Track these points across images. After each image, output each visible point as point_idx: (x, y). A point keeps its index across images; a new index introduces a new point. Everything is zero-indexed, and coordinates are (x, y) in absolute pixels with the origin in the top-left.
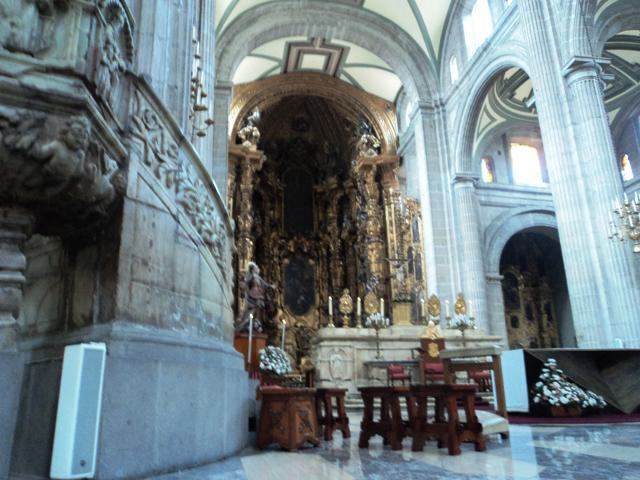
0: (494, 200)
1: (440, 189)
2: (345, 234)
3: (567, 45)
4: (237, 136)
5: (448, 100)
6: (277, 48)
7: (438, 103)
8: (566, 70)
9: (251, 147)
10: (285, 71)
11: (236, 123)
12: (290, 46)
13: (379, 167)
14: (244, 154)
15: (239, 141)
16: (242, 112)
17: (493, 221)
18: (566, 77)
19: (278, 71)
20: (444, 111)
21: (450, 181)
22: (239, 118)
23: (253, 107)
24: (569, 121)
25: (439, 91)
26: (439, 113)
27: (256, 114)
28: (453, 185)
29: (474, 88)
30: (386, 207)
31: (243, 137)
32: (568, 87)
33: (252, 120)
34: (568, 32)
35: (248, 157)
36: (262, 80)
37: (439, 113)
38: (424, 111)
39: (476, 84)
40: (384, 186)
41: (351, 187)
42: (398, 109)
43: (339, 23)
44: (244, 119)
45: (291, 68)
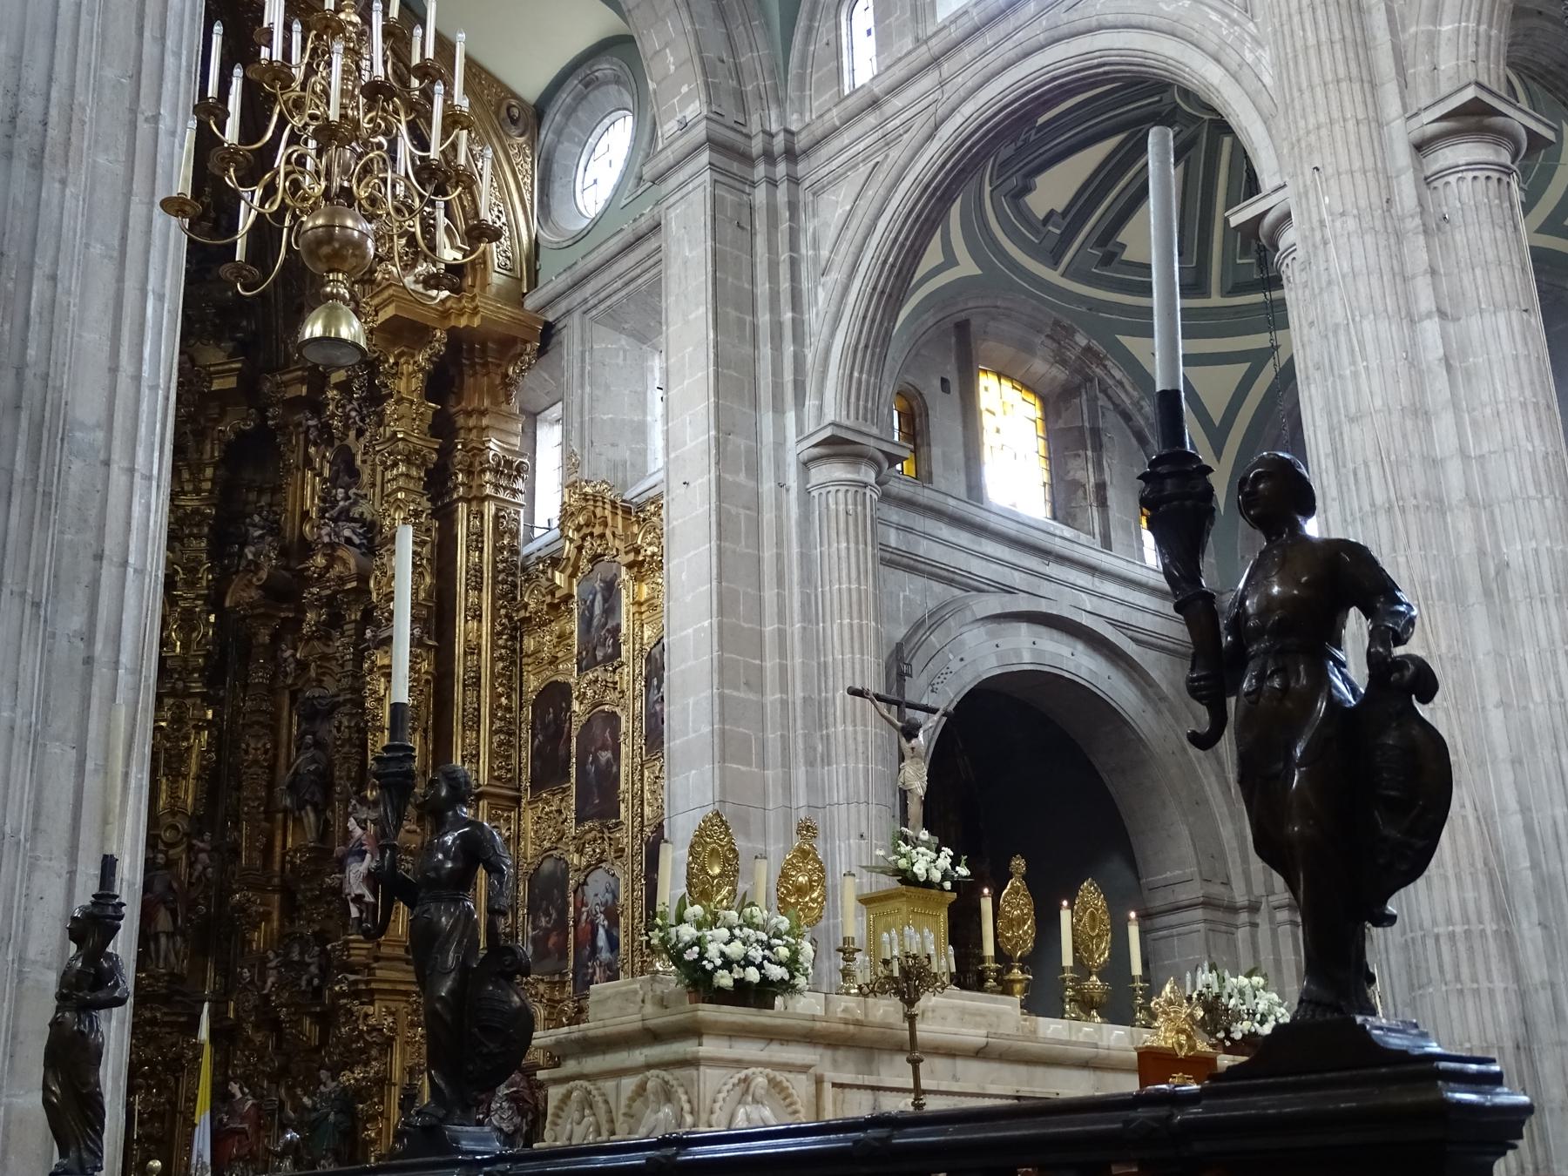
0: (924, 548)
1: (754, 471)
2: (241, 594)
3: (1432, 41)
5: (818, 143)
7: (779, 143)
17: (918, 625)
18: (1421, 147)
20: (794, 181)
21: (794, 450)
24: (1425, 302)
25: (780, 103)
26: (773, 183)
28: (806, 465)
29: (957, 119)
30: (462, 508)
37: (773, 183)
38: (721, 161)
39: (968, 109)
41: (296, 404)
42: (547, 135)
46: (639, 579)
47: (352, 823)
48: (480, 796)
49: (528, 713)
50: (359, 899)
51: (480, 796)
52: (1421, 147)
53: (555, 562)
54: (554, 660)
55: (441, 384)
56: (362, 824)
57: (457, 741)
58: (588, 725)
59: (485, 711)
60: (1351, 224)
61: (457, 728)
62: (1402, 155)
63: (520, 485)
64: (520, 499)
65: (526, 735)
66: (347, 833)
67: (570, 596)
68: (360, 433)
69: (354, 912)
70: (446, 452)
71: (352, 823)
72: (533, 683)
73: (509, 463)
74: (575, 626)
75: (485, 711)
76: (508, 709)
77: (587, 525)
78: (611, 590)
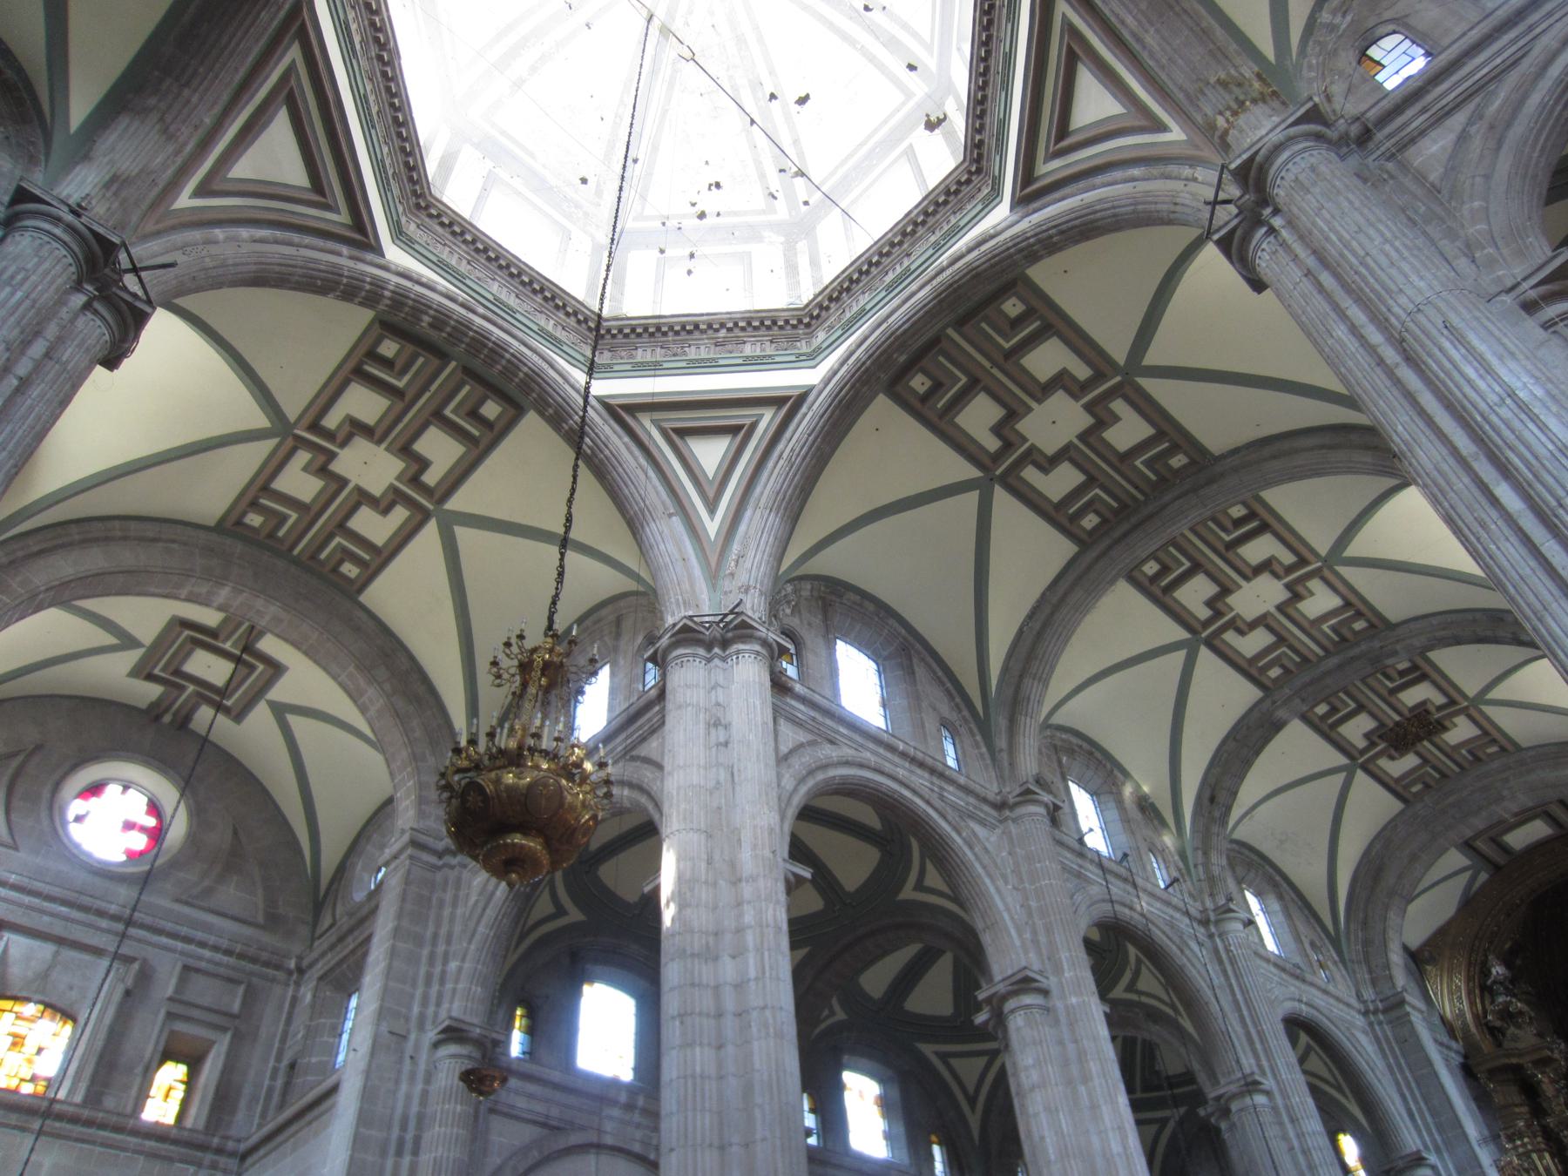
4: (1486, 1025)
6: (1455, 859)
9: (1525, 1037)
10: (1497, 868)
11: (1472, 1004)
12: (1468, 846)
14: (1514, 1061)
15: (1494, 1032)
16: (1469, 979)
19: (1483, 877)
22: (1470, 993)
23: (1486, 957)
27: (1498, 970)
31: (1498, 1024)
33: (1495, 982)
35: (1525, 1061)
36: (1468, 904)
43: (1505, 793)
44: (1482, 987)
45: (1500, 859)
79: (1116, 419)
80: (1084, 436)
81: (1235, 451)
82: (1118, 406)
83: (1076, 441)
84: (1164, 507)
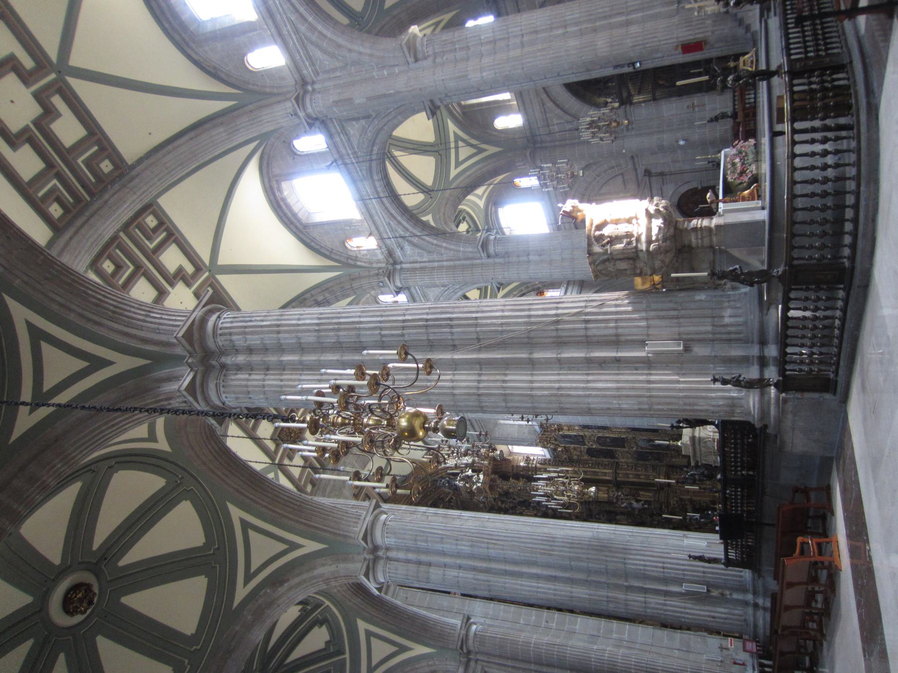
8: (484, 255)
13: (495, 472)
18: (489, 256)
32: (497, 255)
34: (454, 250)
40: (515, 471)
46: (562, 429)
47: (623, 506)
48: (616, 472)
49: (594, 459)
50: (643, 505)
51: (616, 472)
52: (489, 256)
53: (555, 450)
54: (581, 452)
55: (505, 477)
56: (623, 503)
57: (601, 478)
58: (600, 444)
59: (593, 470)
60: (506, 273)
61: (597, 477)
62: (490, 260)
63: (532, 458)
64: (536, 458)
65: (599, 460)
66: (626, 507)
67: (565, 447)
68: (514, 499)
69: (646, 506)
70: (523, 476)
71: (623, 506)
72: (586, 457)
73: (526, 460)
74: (572, 446)
75: (593, 470)
76: (592, 464)
77: (547, 441)
78: (564, 436)
79: (59, 115)
80: (37, 123)
81: (140, 161)
82: (57, 101)
83: (32, 126)
84: (106, 202)
